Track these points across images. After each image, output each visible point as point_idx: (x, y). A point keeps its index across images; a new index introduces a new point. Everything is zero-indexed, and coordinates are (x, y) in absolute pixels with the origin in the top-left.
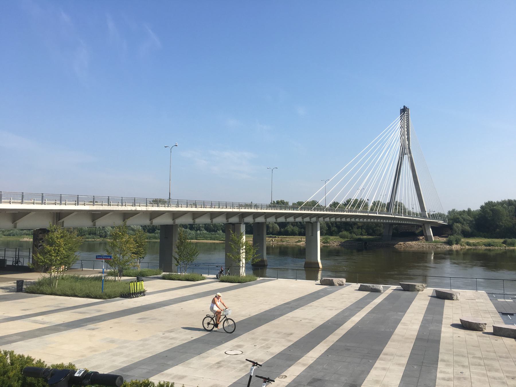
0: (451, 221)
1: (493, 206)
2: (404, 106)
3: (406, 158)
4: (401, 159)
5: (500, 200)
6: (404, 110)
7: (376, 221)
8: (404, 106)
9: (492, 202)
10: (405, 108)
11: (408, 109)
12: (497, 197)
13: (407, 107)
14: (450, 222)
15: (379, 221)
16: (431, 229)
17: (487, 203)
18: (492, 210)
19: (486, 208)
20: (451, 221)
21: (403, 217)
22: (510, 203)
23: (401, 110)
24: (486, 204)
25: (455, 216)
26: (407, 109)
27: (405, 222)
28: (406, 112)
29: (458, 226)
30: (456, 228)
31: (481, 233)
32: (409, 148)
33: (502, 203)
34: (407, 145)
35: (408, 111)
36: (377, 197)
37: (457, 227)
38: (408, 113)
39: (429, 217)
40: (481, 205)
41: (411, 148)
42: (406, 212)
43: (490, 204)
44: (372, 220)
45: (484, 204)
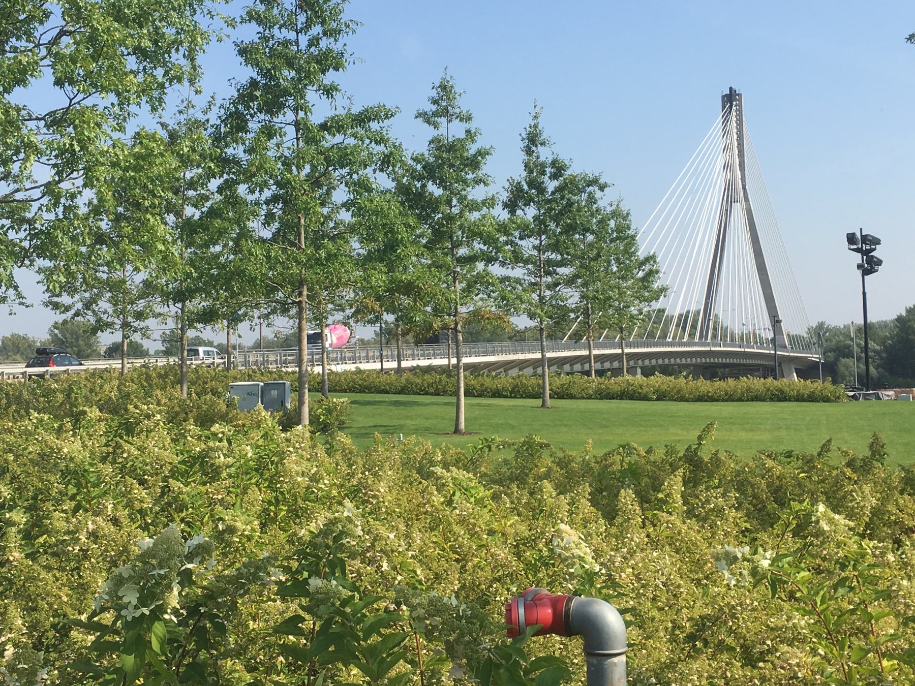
0: (831, 355)
2: (731, 89)
3: (738, 210)
4: (726, 213)
6: (731, 99)
7: (660, 361)
8: (731, 89)
10: (733, 92)
13: (735, 91)
14: (828, 357)
15: (666, 361)
16: (795, 374)
17: (910, 308)
19: (910, 320)
20: (831, 355)
23: (723, 97)
25: (840, 341)
26: (738, 95)
27: (728, 361)
28: (734, 103)
30: (842, 369)
31: (901, 380)
32: (744, 188)
34: (740, 181)
35: (740, 101)
36: (682, 308)
38: (740, 105)
39: (762, 344)
40: (899, 314)
41: (747, 187)
42: (726, 336)
44: (654, 362)
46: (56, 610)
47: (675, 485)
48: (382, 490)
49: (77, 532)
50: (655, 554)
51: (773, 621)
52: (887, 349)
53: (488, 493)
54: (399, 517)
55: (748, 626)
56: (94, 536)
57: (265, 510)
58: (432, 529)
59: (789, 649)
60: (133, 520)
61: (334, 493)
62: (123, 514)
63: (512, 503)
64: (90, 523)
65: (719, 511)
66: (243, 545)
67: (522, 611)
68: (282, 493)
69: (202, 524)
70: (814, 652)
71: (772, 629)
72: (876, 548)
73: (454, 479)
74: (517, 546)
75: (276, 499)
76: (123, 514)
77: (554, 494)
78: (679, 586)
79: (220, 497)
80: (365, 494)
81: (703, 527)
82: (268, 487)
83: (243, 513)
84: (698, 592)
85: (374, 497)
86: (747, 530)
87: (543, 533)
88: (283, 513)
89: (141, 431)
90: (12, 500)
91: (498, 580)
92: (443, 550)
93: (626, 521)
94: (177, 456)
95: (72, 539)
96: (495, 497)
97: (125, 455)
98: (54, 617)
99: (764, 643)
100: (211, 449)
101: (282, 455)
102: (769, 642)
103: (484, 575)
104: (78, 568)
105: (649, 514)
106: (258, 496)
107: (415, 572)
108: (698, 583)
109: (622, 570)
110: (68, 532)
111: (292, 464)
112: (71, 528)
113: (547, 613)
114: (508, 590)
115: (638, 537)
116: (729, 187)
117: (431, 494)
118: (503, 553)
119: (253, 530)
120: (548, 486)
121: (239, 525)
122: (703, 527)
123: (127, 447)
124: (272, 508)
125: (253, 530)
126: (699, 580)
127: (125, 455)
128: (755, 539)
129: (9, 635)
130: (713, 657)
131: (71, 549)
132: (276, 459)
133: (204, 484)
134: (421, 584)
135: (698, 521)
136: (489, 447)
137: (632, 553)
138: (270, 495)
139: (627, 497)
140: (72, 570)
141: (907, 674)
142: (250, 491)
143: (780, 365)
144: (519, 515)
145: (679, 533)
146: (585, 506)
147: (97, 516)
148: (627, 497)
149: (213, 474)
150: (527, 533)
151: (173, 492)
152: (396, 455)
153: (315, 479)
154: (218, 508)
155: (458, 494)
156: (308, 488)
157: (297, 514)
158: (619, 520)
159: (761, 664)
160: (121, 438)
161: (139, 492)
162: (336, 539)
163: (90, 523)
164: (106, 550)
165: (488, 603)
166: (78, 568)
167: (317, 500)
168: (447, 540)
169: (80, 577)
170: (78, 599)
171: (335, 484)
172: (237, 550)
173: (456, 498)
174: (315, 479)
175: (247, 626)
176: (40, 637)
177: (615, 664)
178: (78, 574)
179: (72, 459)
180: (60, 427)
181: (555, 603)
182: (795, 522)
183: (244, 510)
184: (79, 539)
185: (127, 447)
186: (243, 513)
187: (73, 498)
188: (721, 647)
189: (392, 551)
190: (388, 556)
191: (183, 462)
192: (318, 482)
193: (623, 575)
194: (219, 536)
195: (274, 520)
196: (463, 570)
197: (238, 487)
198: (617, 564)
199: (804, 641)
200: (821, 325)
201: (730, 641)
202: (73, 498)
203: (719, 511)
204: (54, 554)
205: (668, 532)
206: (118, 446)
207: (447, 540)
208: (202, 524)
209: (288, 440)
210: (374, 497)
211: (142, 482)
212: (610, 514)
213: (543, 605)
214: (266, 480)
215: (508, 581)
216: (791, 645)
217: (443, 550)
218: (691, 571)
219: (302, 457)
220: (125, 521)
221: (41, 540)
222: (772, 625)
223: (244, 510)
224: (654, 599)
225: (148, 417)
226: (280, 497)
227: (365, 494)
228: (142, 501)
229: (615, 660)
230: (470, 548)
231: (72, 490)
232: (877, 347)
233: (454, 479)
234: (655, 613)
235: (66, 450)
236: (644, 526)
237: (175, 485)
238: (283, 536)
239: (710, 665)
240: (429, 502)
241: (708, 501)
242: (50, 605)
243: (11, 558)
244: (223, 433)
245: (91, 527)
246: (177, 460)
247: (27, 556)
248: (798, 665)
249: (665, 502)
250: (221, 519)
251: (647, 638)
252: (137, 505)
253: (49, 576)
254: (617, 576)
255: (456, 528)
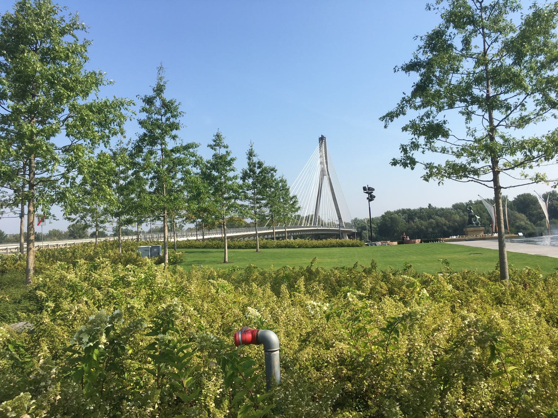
0: (359, 229)
1: (391, 215)
3: (326, 178)
4: (322, 180)
5: (396, 210)
6: (322, 139)
9: (390, 211)
11: (325, 138)
12: (392, 209)
15: (302, 233)
18: (391, 218)
21: (322, 228)
22: (403, 212)
23: (319, 138)
24: (386, 213)
29: (366, 233)
31: (384, 238)
32: (328, 171)
33: (398, 212)
35: (325, 140)
37: (365, 234)
38: (325, 141)
39: (335, 226)
43: (388, 213)
45: (384, 214)
46: (62, 342)
47: (301, 282)
48: (192, 288)
49: (71, 310)
50: (293, 309)
51: (335, 333)
52: (379, 227)
53: (233, 287)
54: (199, 298)
55: (327, 334)
56: (79, 311)
57: (148, 297)
58: (212, 302)
59: (339, 343)
60: (94, 304)
61: (174, 290)
62: (90, 302)
63: (242, 290)
64: (76, 307)
65: (317, 291)
66: (137, 313)
67: (240, 336)
68: (154, 290)
69: (122, 304)
70: (349, 344)
71: (335, 335)
72: (371, 304)
73: (218, 284)
74: (243, 307)
75: (152, 293)
76: (90, 302)
77: (257, 287)
78: (302, 321)
79: (129, 293)
80: (186, 290)
81: (312, 297)
82: (149, 288)
83: (138, 301)
84: (309, 321)
85: (189, 291)
86: (327, 297)
87: (253, 302)
88: (155, 298)
89: (100, 268)
90: (47, 297)
91: (235, 321)
92: (216, 310)
93: (283, 296)
94: (114, 277)
95: (68, 314)
96: (236, 288)
97: (93, 278)
98: (61, 344)
99: (332, 340)
100: (127, 275)
101: (155, 276)
102: (334, 340)
103: (231, 319)
104: (72, 324)
105: (292, 293)
106: (143, 292)
107: (201, 323)
108: (310, 319)
109: (281, 315)
110: (68, 311)
111: (159, 279)
112: (69, 309)
113: (249, 336)
114: (239, 325)
115: (287, 302)
116: (322, 171)
117: (211, 289)
118: (237, 311)
119: (142, 307)
120: (254, 285)
121: (136, 305)
122: (312, 297)
123: (94, 274)
124: (151, 296)
125: (142, 307)
126: (310, 317)
127: (93, 278)
128: (330, 301)
129: (42, 353)
130: (314, 346)
131: (68, 317)
132: (151, 278)
133: (124, 288)
134: (203, 327)
135: (309, 295)
136: (234, 270)
137: (285, 309)
138: (150, 292)
139: (284, 288)
140: (70, 325)
141: (381, 350)
142: (141, 291)
143: (342, 234)
144: (245, 295)
145: (303, 300)
146: (269, 292)
147: (80, 303)
148: (284, 288)
149: (128, 284)
150: (247, 302)
151: (110, 292)
152: (200, 274)
153: (166, 284)
154: (128, 299)
155: (220, 289)
156: (163, 288)
157: (160, 298)
158: (281, 296)
159: (331, 349)
160: (92, 271)
161: (97, 293)
162: (171, 312)
163: (76, 307)
164: (83, 317)
165: (232, 330)
166: (72, 324)
167: (167, 293)
168: (217, 306)
169: (73, 328)
170: (71, 337)
171: (174, 287)
172: (135, 315)
173: (219, 291)
174: (166, 284)
175: (139, 344)
176: (56, 353)
177: (275, 354)
178: (72, 326)
179: (71, 281)
180: (68, 267)
181: (252, 332)
182: (343, 294)
183: (138, 299)
184: (71, 313)
185: (94, 274)
186: (138, 301)
187: (71, 296)
188: (317, 342)
189: (192, 315)
190: (190, 317)
191: (115, 281)
192: (167, 286)
193: (282, 317)
194: (128, 309)
195: (151, 301)
196: (223, 318)
197: (138, 290)
198: (279, 313)
199: (345, 340)
200: (356, 219)
201: (320, 340)
202: (71, 296)
203: (317, 291)
204: (62, 320)
205: (298, 300)
206: (90, 275)
207: (217, 306)
208: (122, 304)
209: (156, 270)
210: (189, 291)
211: (99, 288)
212: (277, 293)
213: (249, 333)
214: (148, 286)
215: (239, 321)
216: (340, 342)
217: (216, 310)
218: (307, 314)
219: (163, 276)
220: (91, 305)
221: (58, 314)
222: (335, 334)
223: (138, 299)
224: (294, 325)
225: (103, 263)
226: (154, 292)
227: (186, 290)
228: (99, 296)
229: (275, 353)
230: (225, 309)
231: (71, 293)
232: (375, 226)
233: (218, 284)
234: (294, 331)
235: (68, 277)
236: (291, 297)
237: (111, 290)
238: (153, 308)
239: (313, 350)
240: (210, 292)
241: (313, 287)
242: (60, 340)
243: (45, 322)
244: (131, 268)
245: (76, 308)
246: (113, 279)
247: (51, 321)
248: (342, 348)
249: (298, 289)
250: (129, 303)
251: (290, 341)
252: (97, 298)
253: (59, 329)
254: (280, 318)
255: (221, 301)
